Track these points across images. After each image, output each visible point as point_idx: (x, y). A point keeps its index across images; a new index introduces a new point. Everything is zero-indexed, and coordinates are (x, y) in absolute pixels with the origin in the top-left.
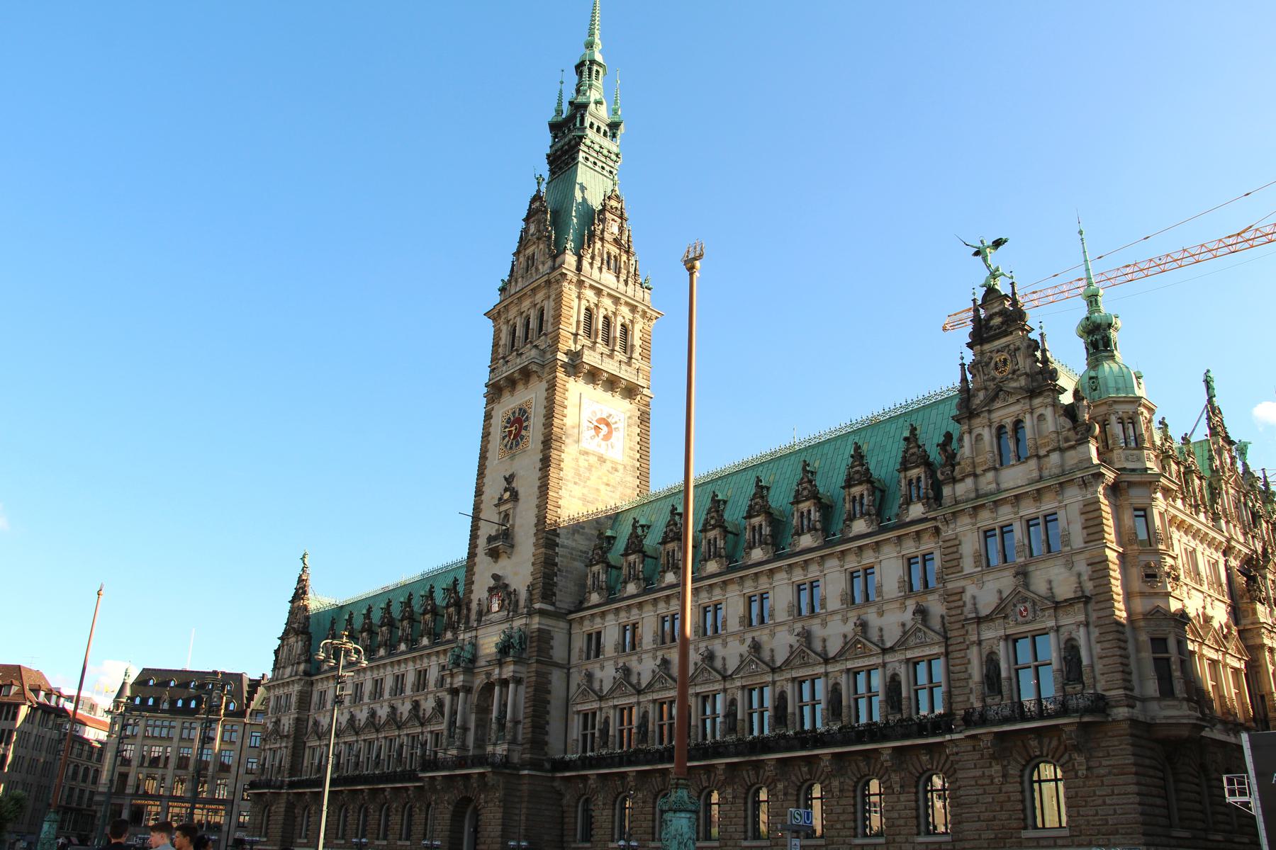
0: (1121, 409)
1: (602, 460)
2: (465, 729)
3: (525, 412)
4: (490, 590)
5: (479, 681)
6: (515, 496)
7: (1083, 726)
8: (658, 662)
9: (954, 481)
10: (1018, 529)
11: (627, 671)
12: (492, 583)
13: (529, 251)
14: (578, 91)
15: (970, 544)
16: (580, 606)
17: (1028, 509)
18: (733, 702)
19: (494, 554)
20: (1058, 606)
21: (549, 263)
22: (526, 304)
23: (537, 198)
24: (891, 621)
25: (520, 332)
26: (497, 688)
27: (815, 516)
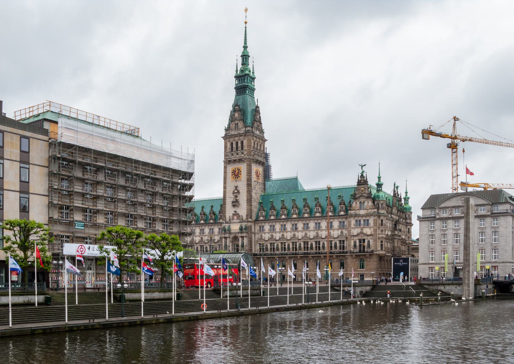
0: (382, 202)
1: (258, 182)
2: (229, 246)
3: (239, 170)
4: (233, 214)
5: (232, 236)
6: (238, 192)
7: (370, 255)
8: (281, 234)
9: (351, 210)
10: (362, 222)
11: (272, 235)
12: (234, 213)
13: (236, 122)
14: (243, 64)
15: (353, 222)
16: (257, 220)
17: (364, 218)
18: (300, 244)
19: (234, 206)
20: (368, 235)
21: (244, 129)
22: (236, 138)
23: (235, 105)
24: (335, 233)
25: (234, 146)
26: (240, 239)
27: (320, 210)
